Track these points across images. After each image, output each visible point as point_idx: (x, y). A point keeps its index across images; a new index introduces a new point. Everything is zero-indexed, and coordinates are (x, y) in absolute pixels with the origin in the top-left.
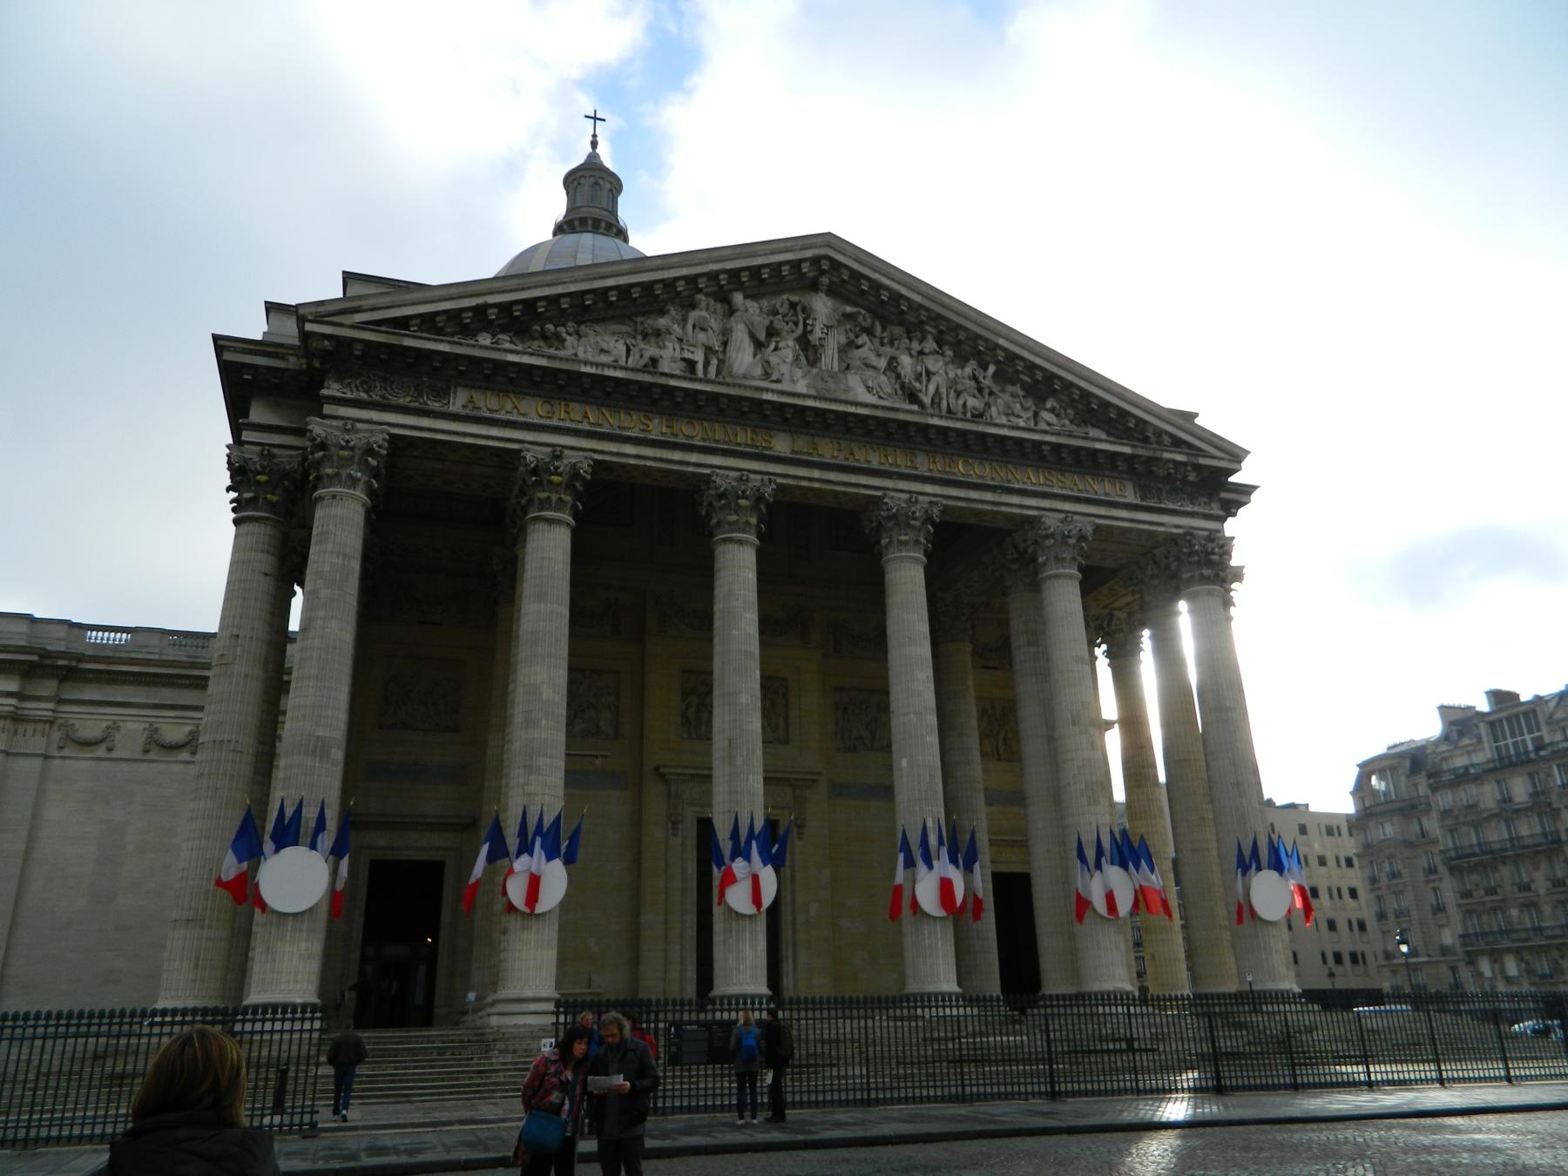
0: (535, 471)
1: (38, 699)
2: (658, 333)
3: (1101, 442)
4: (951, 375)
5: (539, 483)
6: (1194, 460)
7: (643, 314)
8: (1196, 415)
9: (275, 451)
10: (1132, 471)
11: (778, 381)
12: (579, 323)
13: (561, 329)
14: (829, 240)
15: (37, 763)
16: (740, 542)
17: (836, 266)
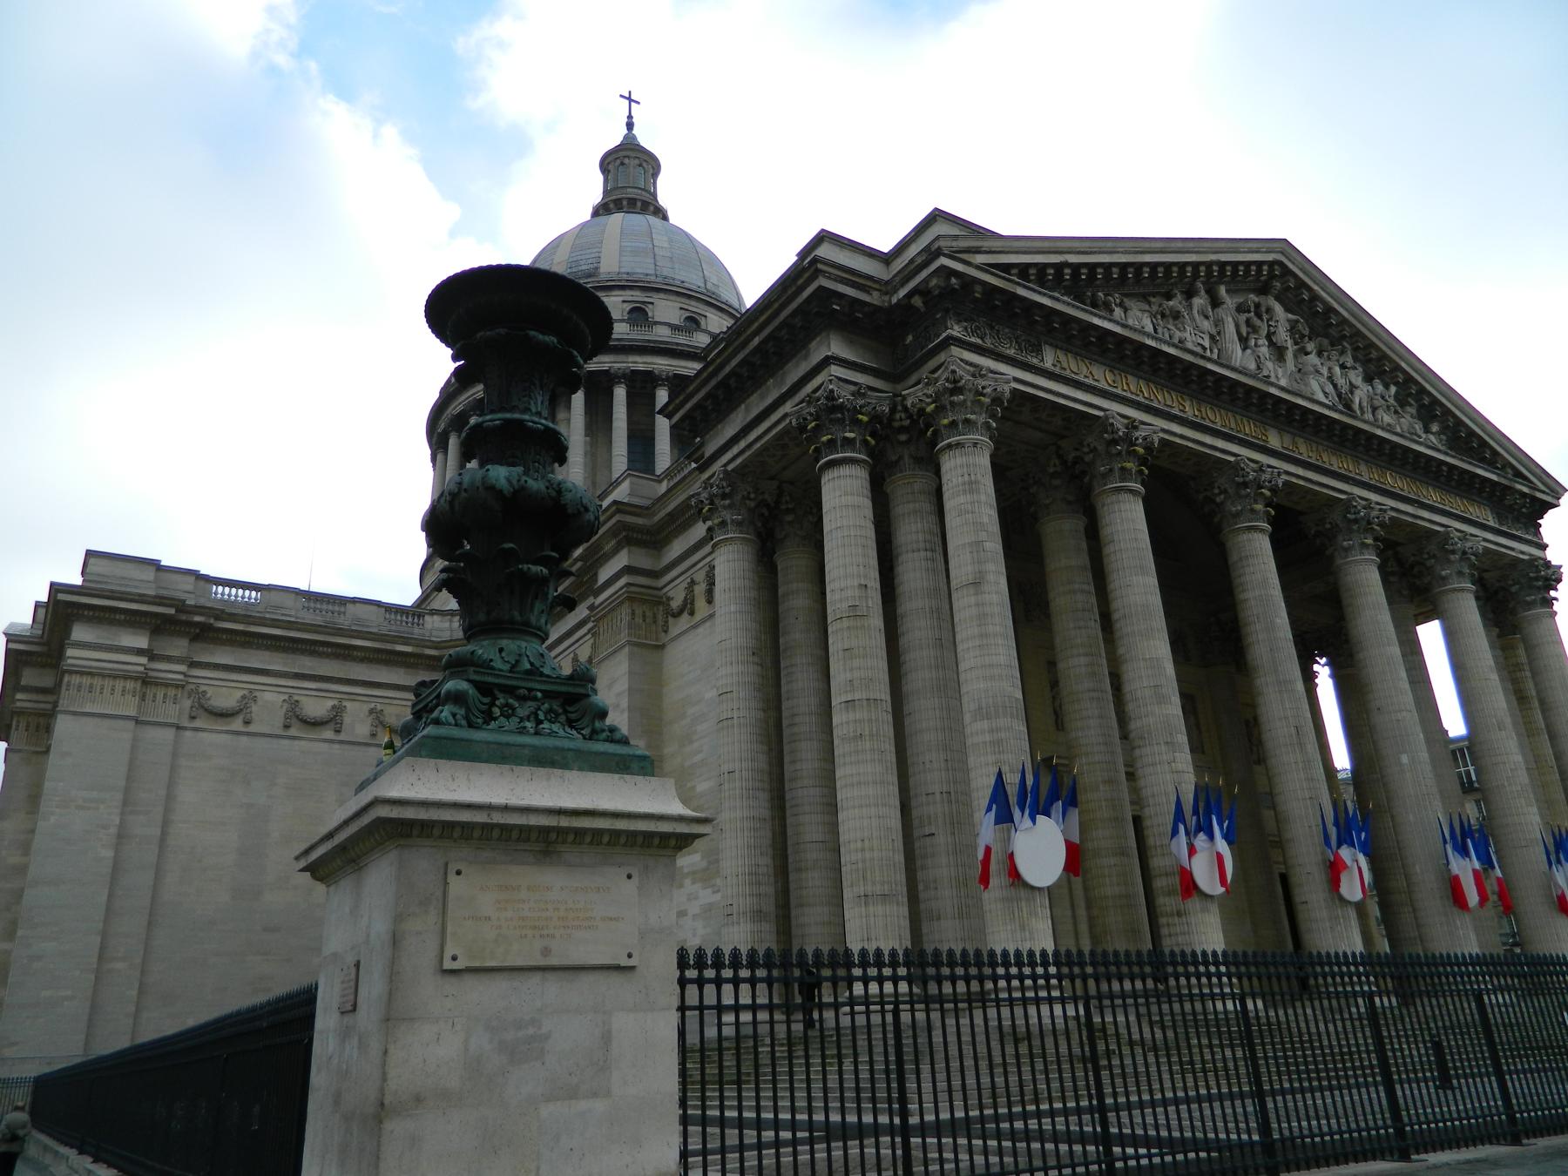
1: (169, 659)
2: (1176, 316)
14: (1284, 246)
15: (169, 734)
16: (1262, 531)
17: (1287, 272)
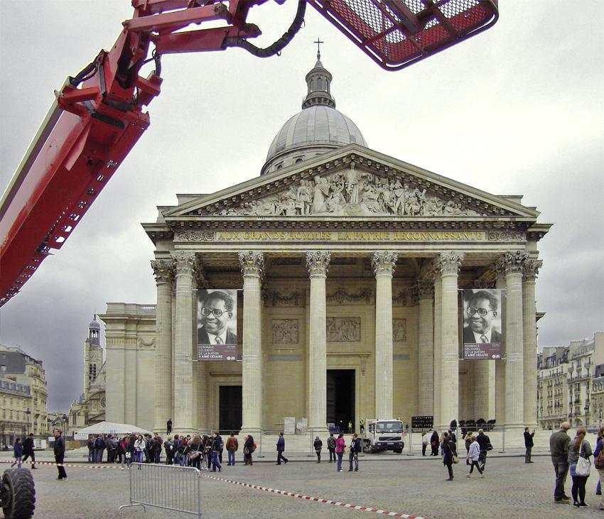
0: (244, 260)
1: (131, 331)
2: (286, 199)
3: (472, 216)
6: (513, 220)
7: (281, 191)
9: (164, 260)
11: (332, 212)
12: (257, 200)
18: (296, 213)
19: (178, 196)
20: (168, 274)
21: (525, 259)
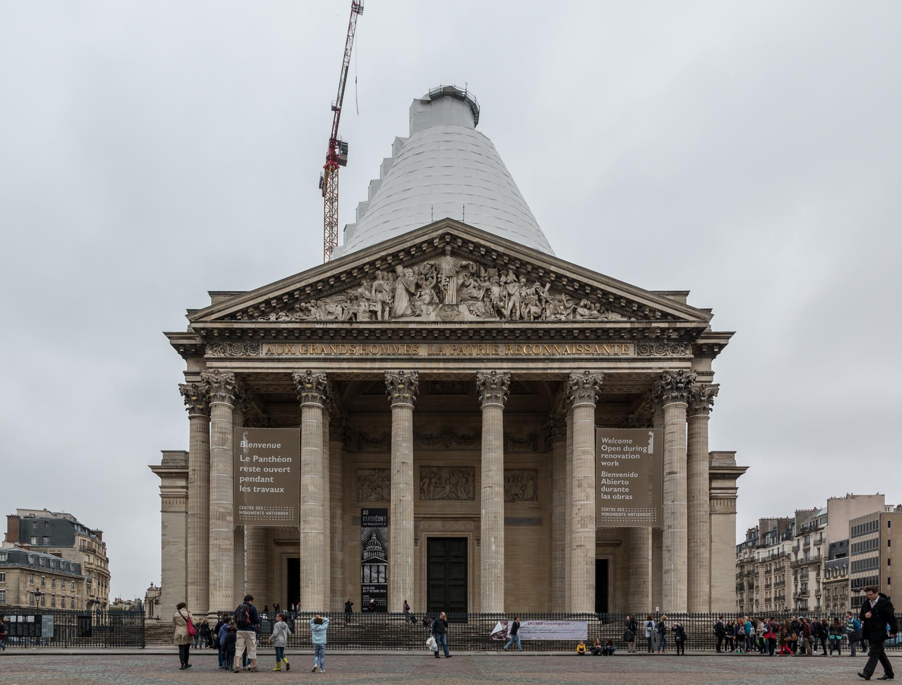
0: (300, 383)
2: (356, 298)
3: (615, 320)
4: (523, 294)
5: (303, 388)
7: (350, 288)
8: (686, 293)
10: (633, 338)
11: (419, 315)
12: (317, 300)
13: (308, 305)
18: (371, 317)
19: (212, 294)
20: (203, 403)
21: (689, 382)
